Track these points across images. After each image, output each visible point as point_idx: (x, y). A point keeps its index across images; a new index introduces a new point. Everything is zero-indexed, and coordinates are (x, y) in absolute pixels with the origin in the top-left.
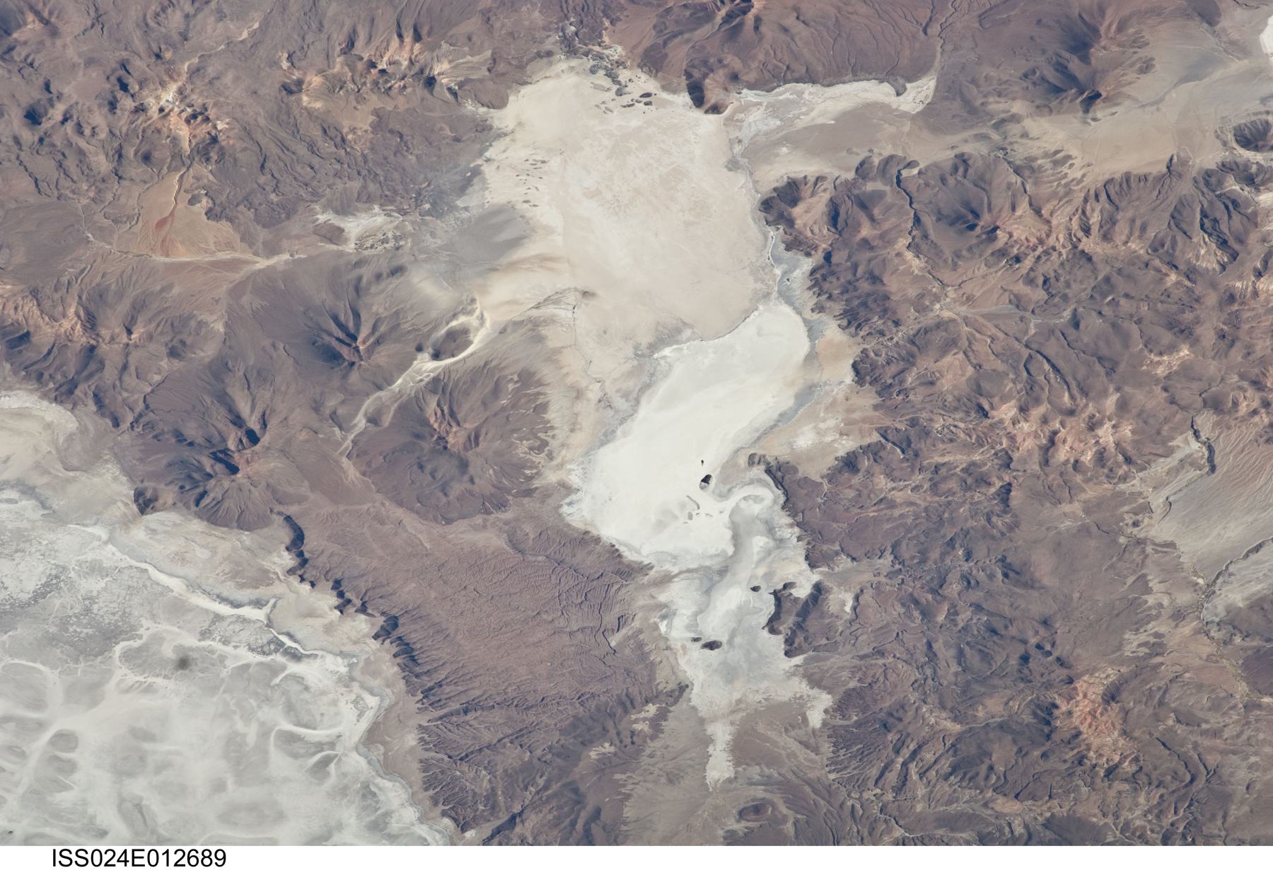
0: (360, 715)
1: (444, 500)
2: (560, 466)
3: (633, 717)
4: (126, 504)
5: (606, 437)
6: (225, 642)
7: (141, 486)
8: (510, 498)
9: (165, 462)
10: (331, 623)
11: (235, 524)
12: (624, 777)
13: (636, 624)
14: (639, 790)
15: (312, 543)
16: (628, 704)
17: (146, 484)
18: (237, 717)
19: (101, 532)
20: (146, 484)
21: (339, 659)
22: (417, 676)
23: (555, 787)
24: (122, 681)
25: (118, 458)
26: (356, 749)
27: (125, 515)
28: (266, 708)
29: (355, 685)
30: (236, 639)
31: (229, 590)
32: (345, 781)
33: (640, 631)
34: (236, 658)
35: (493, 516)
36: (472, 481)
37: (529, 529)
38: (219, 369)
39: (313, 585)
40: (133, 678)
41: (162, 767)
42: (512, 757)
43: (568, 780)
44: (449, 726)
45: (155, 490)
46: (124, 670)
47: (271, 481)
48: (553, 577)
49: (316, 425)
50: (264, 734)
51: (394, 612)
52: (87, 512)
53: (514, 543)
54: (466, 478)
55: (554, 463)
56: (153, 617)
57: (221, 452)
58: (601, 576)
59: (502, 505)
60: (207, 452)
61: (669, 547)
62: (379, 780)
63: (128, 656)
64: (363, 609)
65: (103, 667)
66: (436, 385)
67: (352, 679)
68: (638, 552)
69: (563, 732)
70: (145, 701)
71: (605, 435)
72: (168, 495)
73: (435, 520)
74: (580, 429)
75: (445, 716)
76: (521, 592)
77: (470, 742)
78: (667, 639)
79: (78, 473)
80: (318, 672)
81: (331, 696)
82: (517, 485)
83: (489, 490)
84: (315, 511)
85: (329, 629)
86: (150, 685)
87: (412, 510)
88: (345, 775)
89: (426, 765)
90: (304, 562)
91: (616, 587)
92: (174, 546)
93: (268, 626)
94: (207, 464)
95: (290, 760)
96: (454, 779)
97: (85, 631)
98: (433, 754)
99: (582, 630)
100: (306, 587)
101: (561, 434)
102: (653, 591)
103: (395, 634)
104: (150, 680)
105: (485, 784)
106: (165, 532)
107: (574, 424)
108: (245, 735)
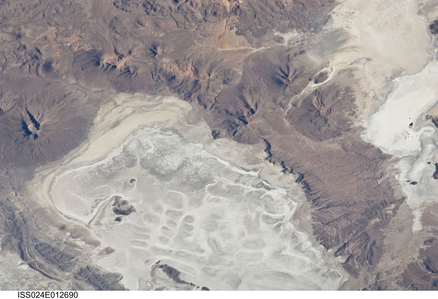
0: (291, 209)
1: (319, 133)
2: (360, 120)
3: (387, 209)
4: (209, 136)
5: (376, 110)
6: (244, 184)
7: (214, 129)
8: (342, 132)
9: (222, 121)
10: (281, 177)
11: (247, 142)
12: (383, 230)
13: (387, 176)
14: (389, 235)
15: (274, 148)
16: (385, 204)
17: (216, 128)
18: (248, 210)
19: (200, 145)
20: (216, 128)
21: (284, 189)
22: (311, 195)
23: (359, 234)
24: (209, 198)
25: (206, 119)
26: (290, 221)
27: (209, 139)
28: (258, 207)
29: (289, 199)
30: (248, 183)
31: (245, 165)
32: (286, 232)
33: (389, 178)
34: (248, 189)
35: (337, 138)
36: (329, 126)
37: (349, 143)
38: (241, 88)
39: (274, 163)
40: (212, 197)
41: (223, 228)
42: (344, 223)
43: (364, 231)
44: (322, 213)
45: (219, 130)
46: (209, 194)
47: (259, 127)
48: (358, 160)
49: (274, 107)
50: (258, 216)
51: (302, 173)
52: (195, 139)
53: (344, 148)
54: (327, 125)
55: (358, 119)
56: (219, 175)
57: (241, 117)
58: (374, 159)
59: (339, 135)
60: (237, 117)
61: (399, 149)
62: (298, 232)
63: (210, 189)
64: (292, 172)
65: (202, 193)
66: (316, 92)
67: (288, 196)
68: (387, 150)
69: (362, 214)
70: (217, 205)
71: (375, 109)
72: (224, 132)
73: (316, 140)
74: (367, 107)
75: (321, 209)
76: (346, 165)
77: (329, 218)
78: (398, 181)
79: (192, 125)
80: (276, 194)
81: (281, 202)
82: (344, 127)
83: (335, 129)
84: (274, 137)
85: (280, 179)
86: (218, 199)
87: (308, 137)
88: (286, 230)
89: (314, 226)
90: (271, 155)
91: (380, 163)
92: (226, 150)
93: (259, 177)
94: (237, 121)
95: (267, 225)
96: (324, 231)
97: (196, 180)
98: (316, 222)
99: (368, 178)
100: (272, 164)
101: (360, 108)
102: (393, 164)
103: (303, 180)
104: (218, 197)
105: (335, 233)
106: (223, 145)
107: (364, 105)
108: (251, 216)
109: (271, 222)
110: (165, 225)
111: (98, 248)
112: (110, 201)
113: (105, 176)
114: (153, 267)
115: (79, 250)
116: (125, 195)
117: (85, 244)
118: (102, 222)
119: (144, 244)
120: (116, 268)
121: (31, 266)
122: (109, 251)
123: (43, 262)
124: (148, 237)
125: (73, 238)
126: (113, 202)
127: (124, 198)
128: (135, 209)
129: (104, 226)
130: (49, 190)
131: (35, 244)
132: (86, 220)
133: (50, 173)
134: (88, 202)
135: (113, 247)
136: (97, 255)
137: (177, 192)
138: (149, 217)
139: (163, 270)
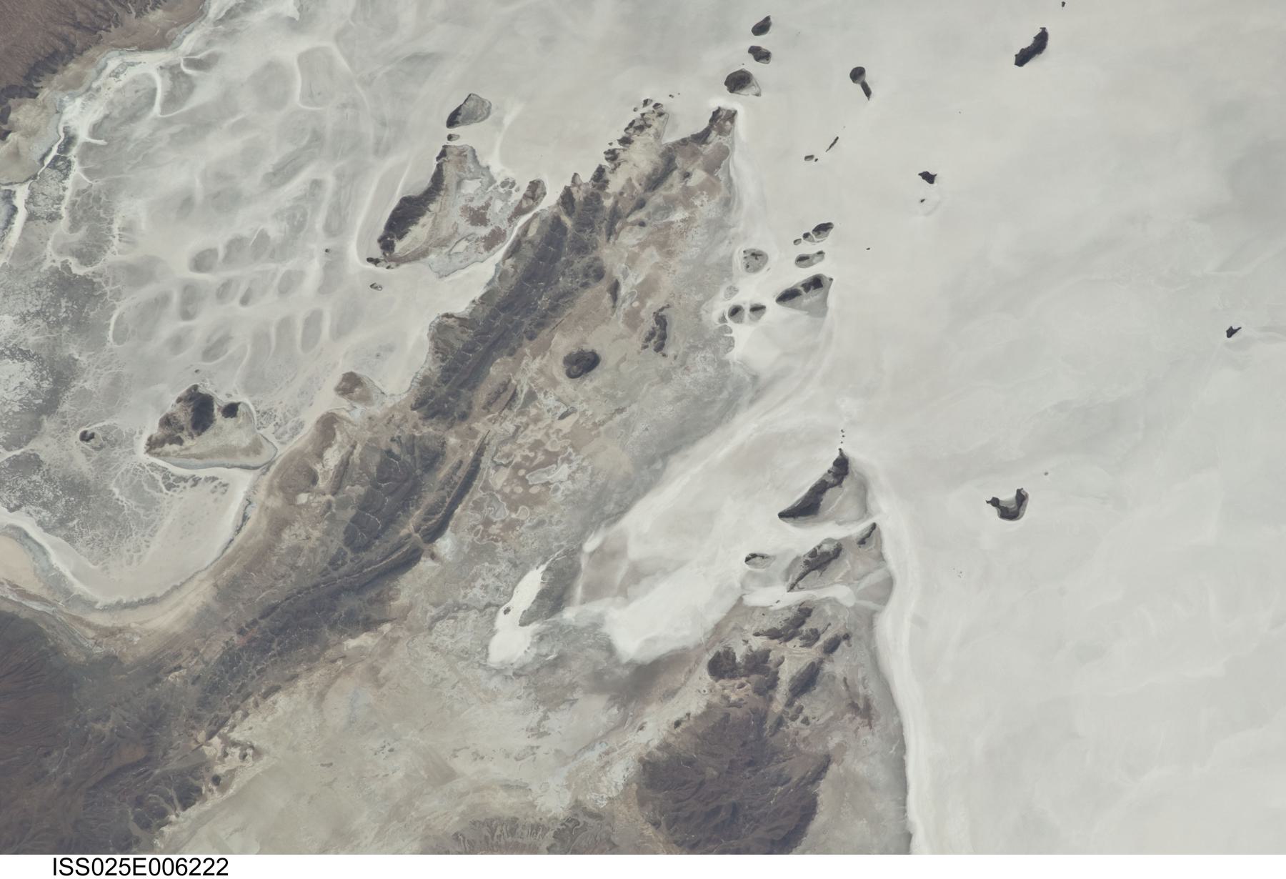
18: (151, 151)
50: (169, 122)
70: (143, 226)
104: (116, 232)
109: (185, 86)
110: (236, 303)
111: (343, 413)
112: (167, 454)
113: (79, 503)
114: (393, 264)
115: (359, 448)
116: (141, 433)
117: (335, 447)
118: (246, 442)
119: (313, 321)
120: (411, 343)
121: (435, 533)
122: (351, 385)
123: (418, 513)
124: (285, 324)
125: (314, 480)
126: (175, 447)
127: (152, 428)
128: (189, 390)
129: (262, 431)
130: (152, 601)
131: (350, 555)
132: (242, 482)
133: (89, 625)
134: (176, 504)
135: (335, 379)
136: (373, 404)
137: (112, 327)
138: (212, 351)
139: (400, 238)
